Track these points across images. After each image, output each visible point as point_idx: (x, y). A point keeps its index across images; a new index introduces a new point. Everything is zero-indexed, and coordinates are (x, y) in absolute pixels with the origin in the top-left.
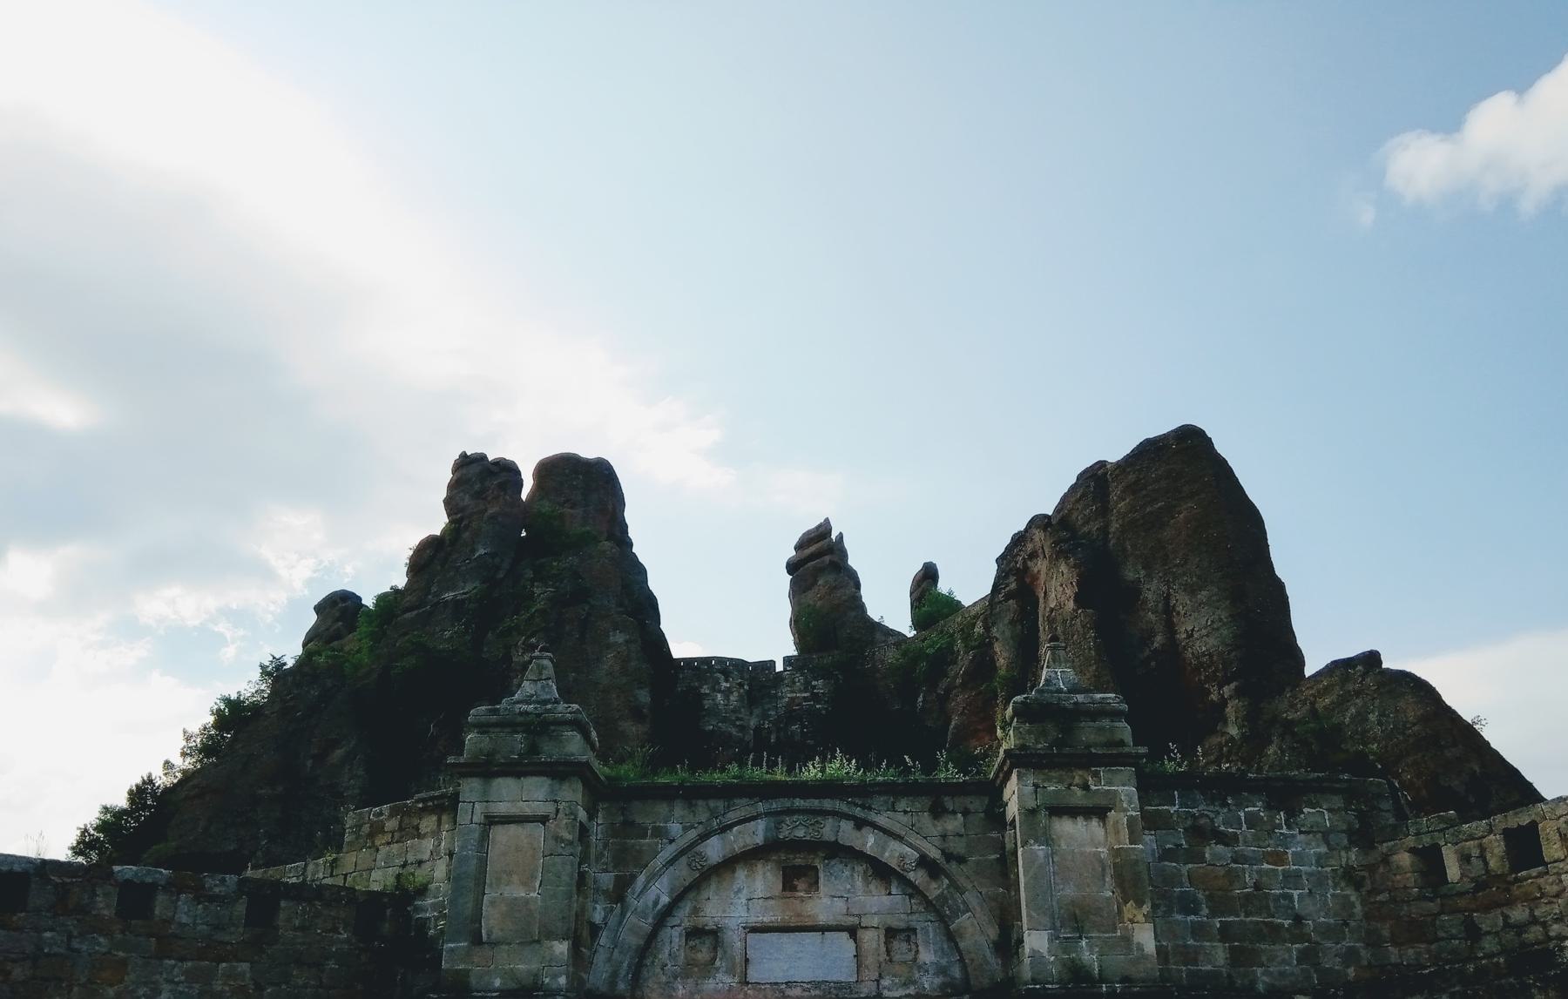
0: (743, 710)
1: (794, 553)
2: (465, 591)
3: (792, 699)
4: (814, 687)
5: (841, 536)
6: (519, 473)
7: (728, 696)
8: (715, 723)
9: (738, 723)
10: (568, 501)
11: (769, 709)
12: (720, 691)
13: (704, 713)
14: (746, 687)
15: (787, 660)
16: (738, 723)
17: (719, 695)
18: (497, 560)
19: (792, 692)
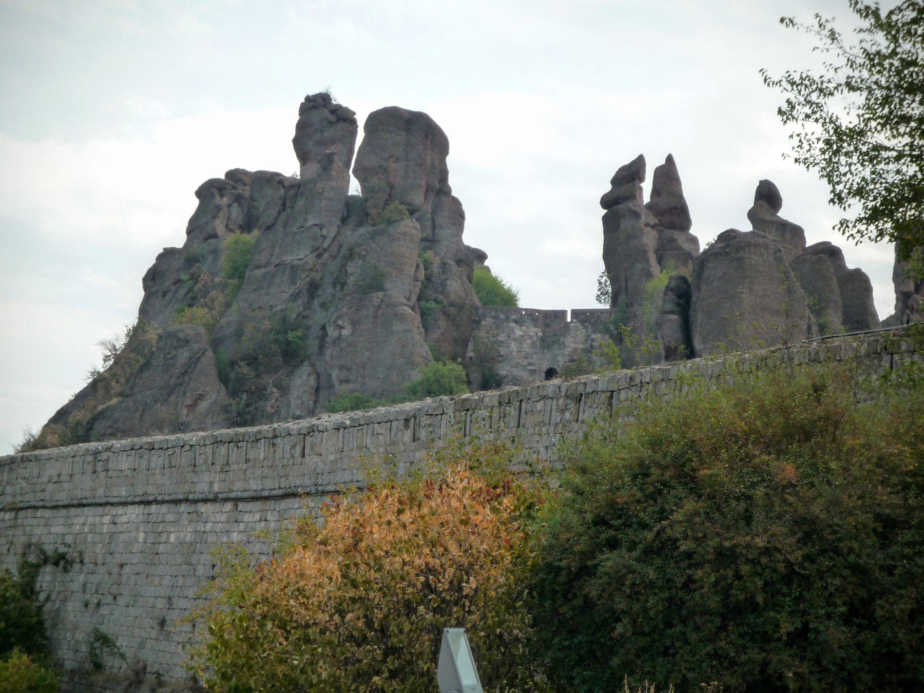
0: (534, 356)
1: (608, 188)
2: (299, 257)
3: (575, 349)
4: (593, 340)
5: (670, 159)
6: (353, 123)
7: (522, 343)
8: (508, 368)
9: (529, 368)
10: (392, 156)
11: (557, 356)
12: (515, 340)
13: (500, 359)
14: (540, 334)
15: (575, 313)
16: (529, 368)
17: (513, 344)
18: (324, 232)
19: (575, 343)
